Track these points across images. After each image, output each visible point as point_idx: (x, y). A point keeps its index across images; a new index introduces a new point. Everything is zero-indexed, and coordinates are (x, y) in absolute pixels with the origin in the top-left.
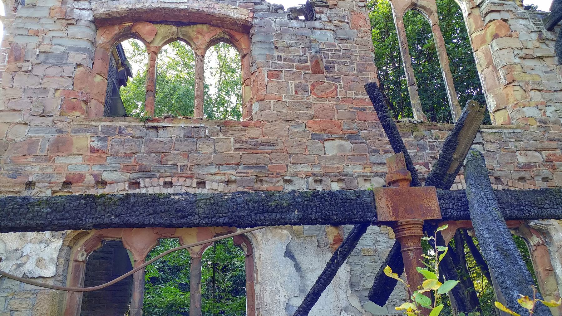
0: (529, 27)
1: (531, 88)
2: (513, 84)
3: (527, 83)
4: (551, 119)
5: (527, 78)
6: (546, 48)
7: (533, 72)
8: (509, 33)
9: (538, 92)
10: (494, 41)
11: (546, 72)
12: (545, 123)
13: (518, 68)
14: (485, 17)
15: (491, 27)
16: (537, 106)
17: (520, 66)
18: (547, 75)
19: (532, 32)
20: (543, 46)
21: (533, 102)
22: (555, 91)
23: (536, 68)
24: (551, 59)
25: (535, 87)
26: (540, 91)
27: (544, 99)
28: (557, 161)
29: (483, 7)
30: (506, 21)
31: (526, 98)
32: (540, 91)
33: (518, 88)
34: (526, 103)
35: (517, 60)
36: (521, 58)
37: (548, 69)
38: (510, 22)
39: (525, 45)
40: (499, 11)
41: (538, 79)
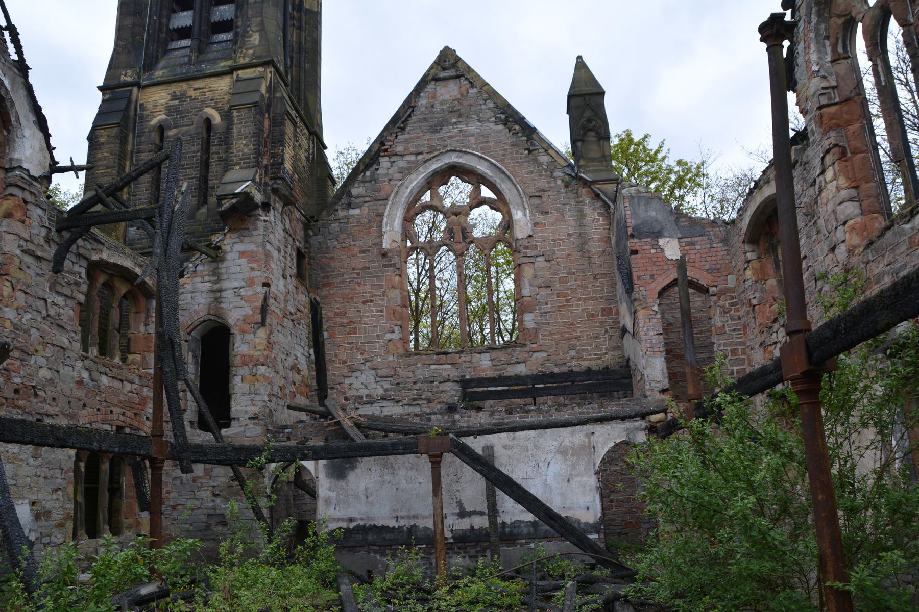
0: (43, 220)
1: (19, 288)
2: (7, 277)
3: (18, 281)
4: (25, 327)
5: (20, 275)
6: (48, 248)
7: (28, 271)
8: (23, 218)
9: (23, 295)
10: (7, 219)
11: (38, 274)
12: (18, 330)
13: (17, 260)
14: (7, 186)
15: (10, 202)
16: (17, 309)
17: (19, 260)
18: (39, 278)
19: (43, 226)
20: (47, 247)
21: (16, 304)
22: (38, 298)
23: (32, 266)
24: (47, 263)
25: (24, 288)
26: (26, 293)
27: (26, 303)
28: (14, 371)
29: (10, 174)
30: (26, 202)
31: (12, 297)
32: (26, 293)
33: (8, 284)
34: (9, 303)
35: (18, 252)
36: (23, 251)
37: (40, 272)
38: (29, 206)
39: (32, 238)
40: (23, 189)
41: (29, 281)
